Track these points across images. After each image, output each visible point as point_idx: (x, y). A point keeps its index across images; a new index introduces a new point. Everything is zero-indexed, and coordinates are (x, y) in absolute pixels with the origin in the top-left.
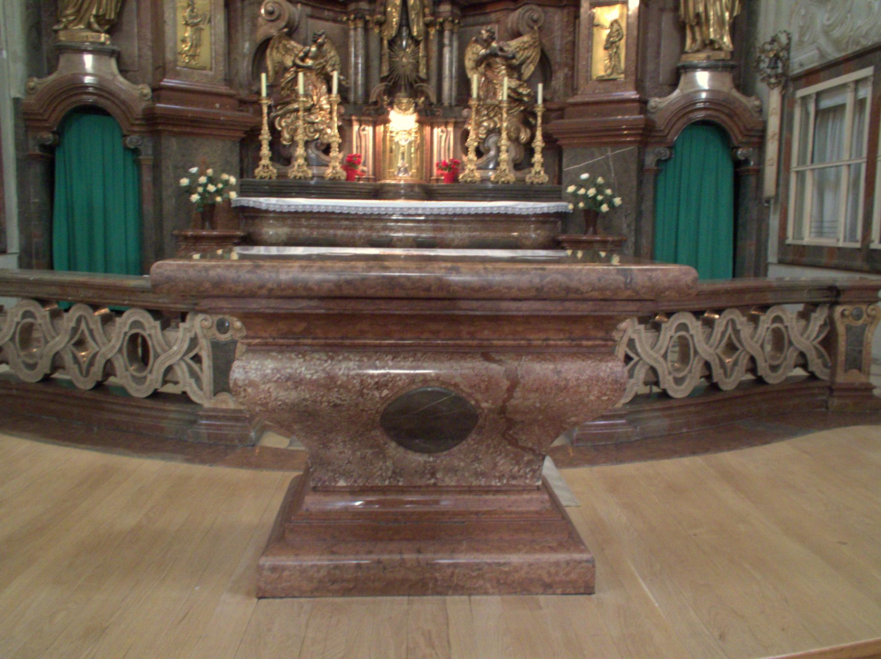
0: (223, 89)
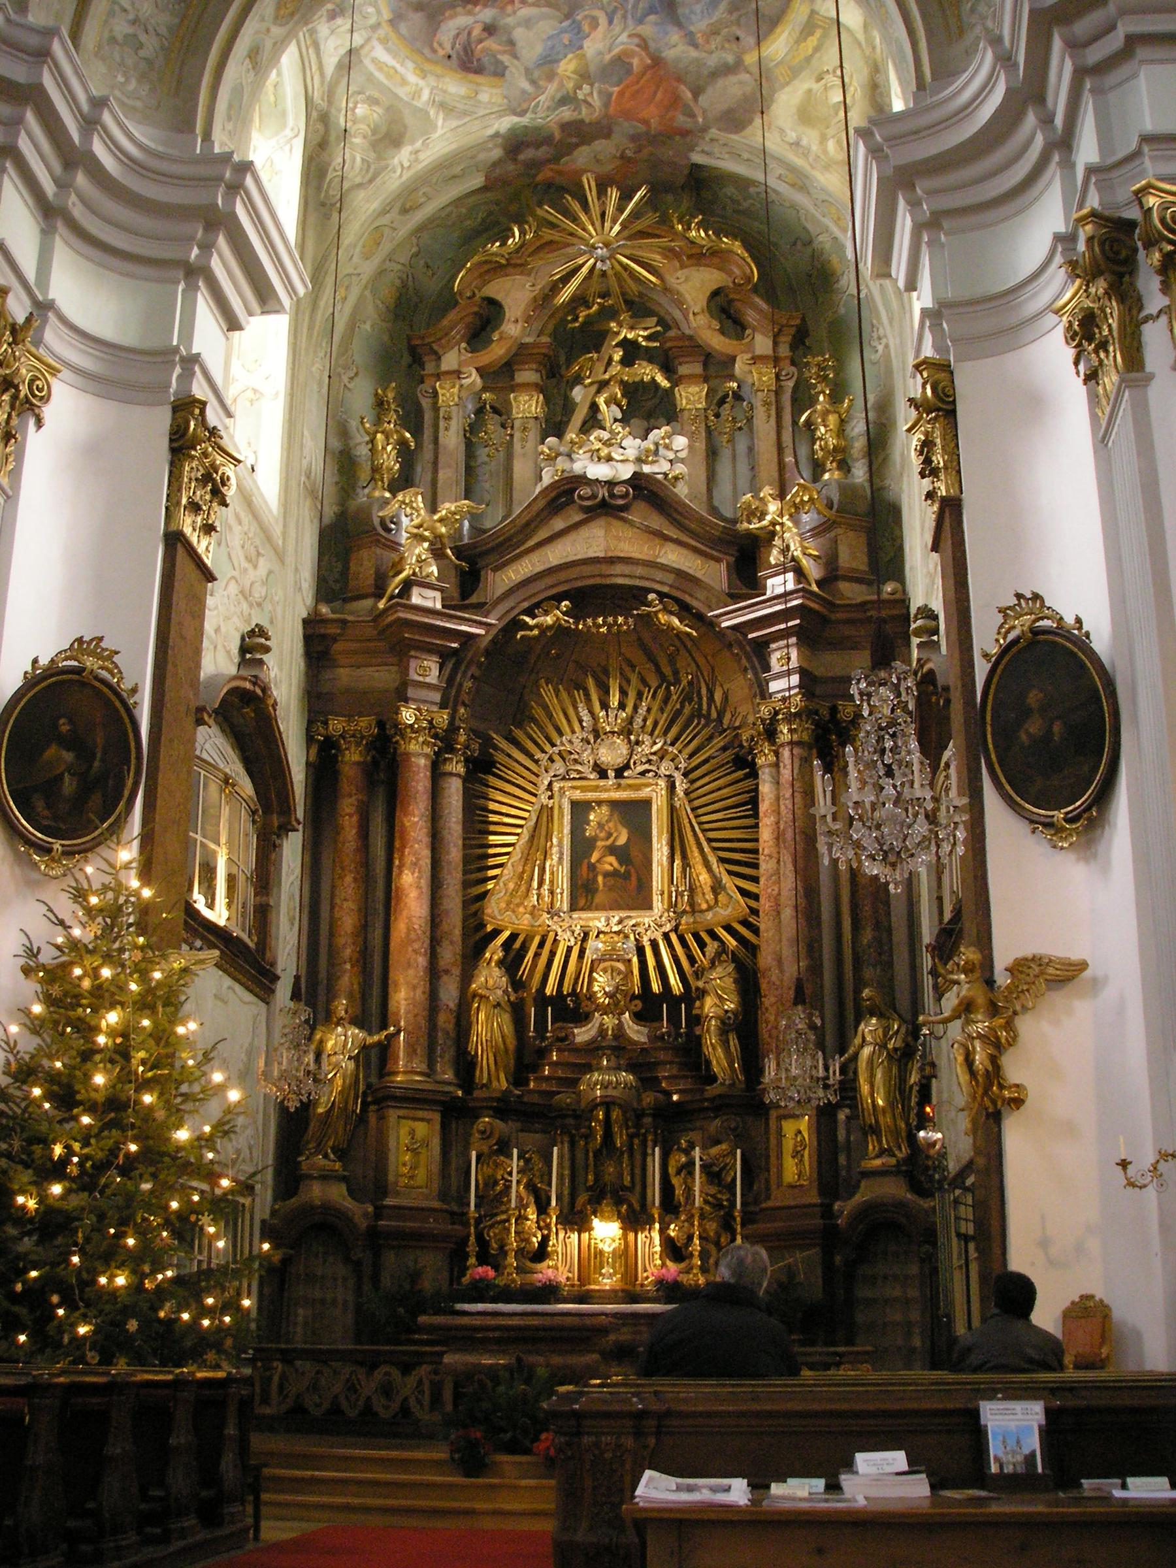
0: (436, 1204)
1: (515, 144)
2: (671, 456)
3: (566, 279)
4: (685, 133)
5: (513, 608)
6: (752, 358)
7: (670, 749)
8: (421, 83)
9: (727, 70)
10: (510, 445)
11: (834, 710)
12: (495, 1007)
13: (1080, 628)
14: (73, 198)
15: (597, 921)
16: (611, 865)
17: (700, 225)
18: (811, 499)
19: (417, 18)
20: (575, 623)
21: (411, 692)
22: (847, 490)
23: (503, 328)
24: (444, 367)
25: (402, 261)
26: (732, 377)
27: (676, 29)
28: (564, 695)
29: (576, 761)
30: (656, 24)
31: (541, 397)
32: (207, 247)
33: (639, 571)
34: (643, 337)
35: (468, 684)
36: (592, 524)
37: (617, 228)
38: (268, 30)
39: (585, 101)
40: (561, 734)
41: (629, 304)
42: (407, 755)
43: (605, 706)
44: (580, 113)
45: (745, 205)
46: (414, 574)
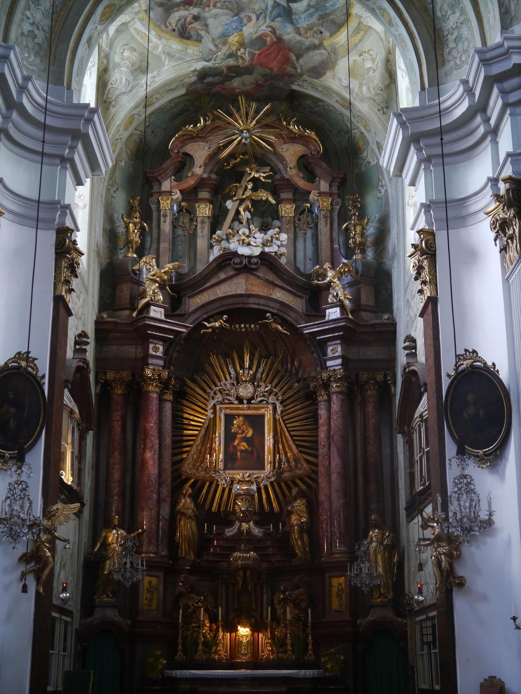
1: (203, 75)
2: (279, 243)
3: (226, 146)
4: (290, 76)
5: (198, 318)
6: (319, 193)
7: (274, 390)
8: (159, 42)
9: (315, 47)
10: (195, 230)
11: (357, 375)
12: (188, 518)
13: (494, 368)
14: (11, 124)
15: (238, 475)
16: (244, 446)
17: (295, 123)
18: (349, 270)
19: (160, 10)
20: (230, 327)
21: (151, 361)
22: (366, 265)
23: (193, 170)
24: (163, 189)
25: (141, 129)
26: (308, 201)
27: (290, 25)
28: (222, 361)
29: (227, 394)
30: (281, 22)
31: (211, 206)
32: (73, 148)
33: (262, 301)
34: (263, 177)
35: (175, 355)
36: (240, 277)
37: (254, 122)
38: (96, 28)
39: (242, 57)
40: (220, 381)
41: (256, 158)
42: (148, 392)
43: (242, 367)
44: (238, 62)
45: (316, 109)
46: (152, 300)
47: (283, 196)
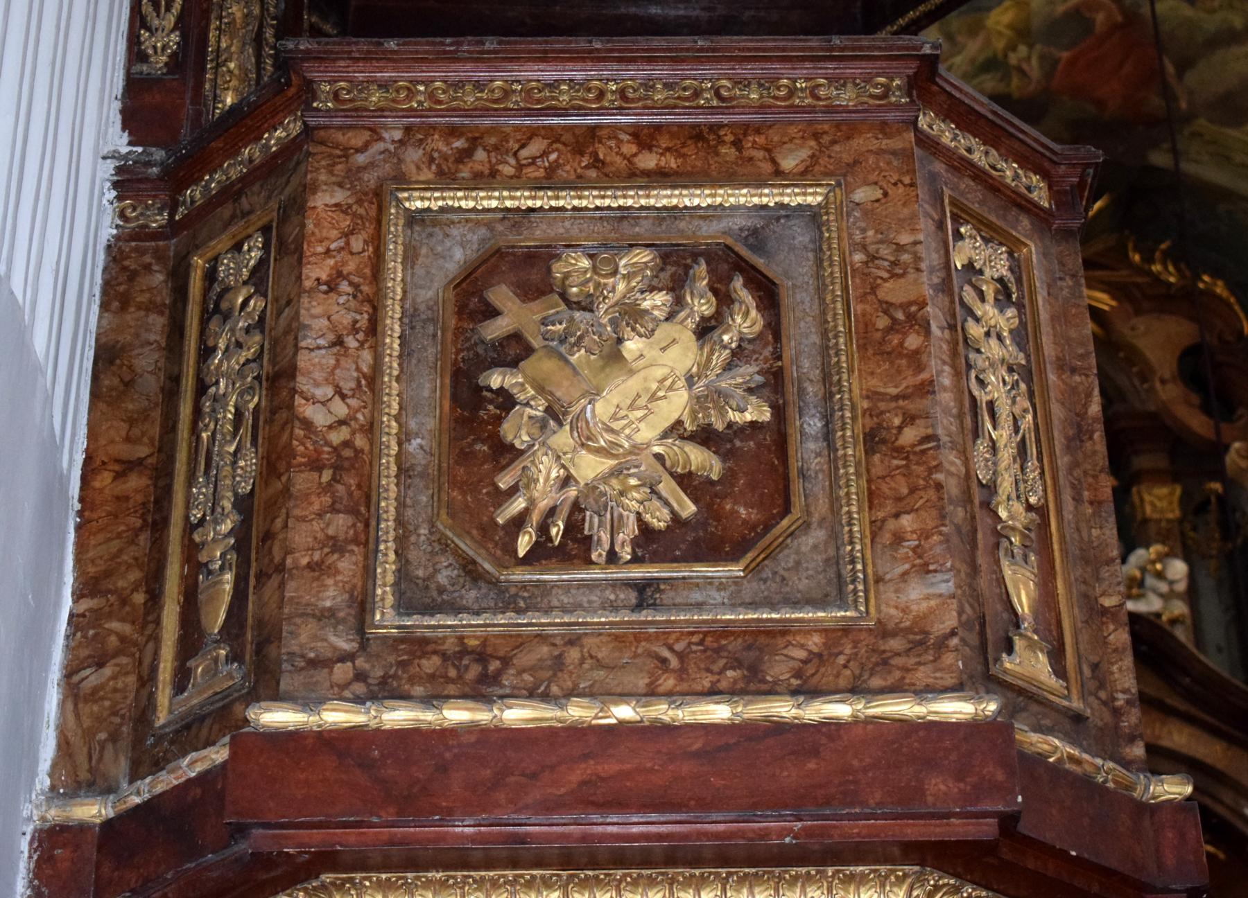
17: (1166, 256)
47: (1143, 462)
